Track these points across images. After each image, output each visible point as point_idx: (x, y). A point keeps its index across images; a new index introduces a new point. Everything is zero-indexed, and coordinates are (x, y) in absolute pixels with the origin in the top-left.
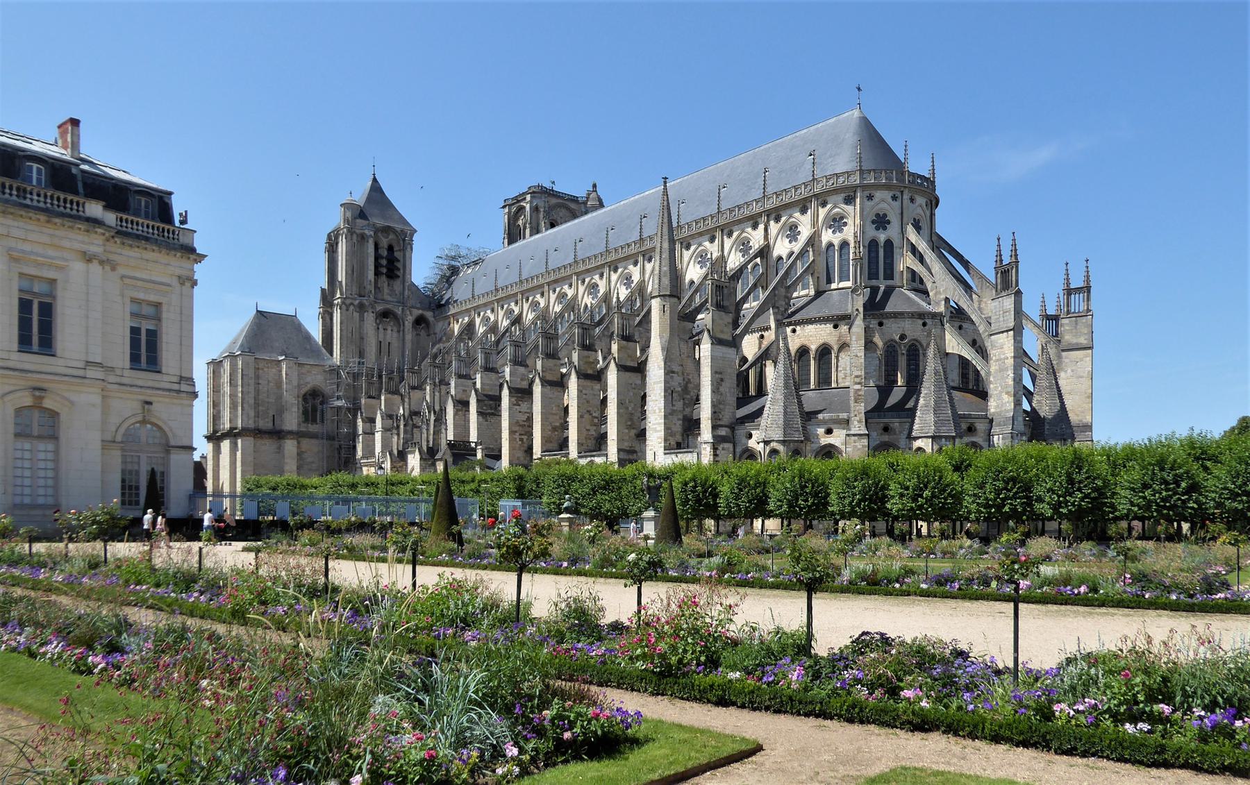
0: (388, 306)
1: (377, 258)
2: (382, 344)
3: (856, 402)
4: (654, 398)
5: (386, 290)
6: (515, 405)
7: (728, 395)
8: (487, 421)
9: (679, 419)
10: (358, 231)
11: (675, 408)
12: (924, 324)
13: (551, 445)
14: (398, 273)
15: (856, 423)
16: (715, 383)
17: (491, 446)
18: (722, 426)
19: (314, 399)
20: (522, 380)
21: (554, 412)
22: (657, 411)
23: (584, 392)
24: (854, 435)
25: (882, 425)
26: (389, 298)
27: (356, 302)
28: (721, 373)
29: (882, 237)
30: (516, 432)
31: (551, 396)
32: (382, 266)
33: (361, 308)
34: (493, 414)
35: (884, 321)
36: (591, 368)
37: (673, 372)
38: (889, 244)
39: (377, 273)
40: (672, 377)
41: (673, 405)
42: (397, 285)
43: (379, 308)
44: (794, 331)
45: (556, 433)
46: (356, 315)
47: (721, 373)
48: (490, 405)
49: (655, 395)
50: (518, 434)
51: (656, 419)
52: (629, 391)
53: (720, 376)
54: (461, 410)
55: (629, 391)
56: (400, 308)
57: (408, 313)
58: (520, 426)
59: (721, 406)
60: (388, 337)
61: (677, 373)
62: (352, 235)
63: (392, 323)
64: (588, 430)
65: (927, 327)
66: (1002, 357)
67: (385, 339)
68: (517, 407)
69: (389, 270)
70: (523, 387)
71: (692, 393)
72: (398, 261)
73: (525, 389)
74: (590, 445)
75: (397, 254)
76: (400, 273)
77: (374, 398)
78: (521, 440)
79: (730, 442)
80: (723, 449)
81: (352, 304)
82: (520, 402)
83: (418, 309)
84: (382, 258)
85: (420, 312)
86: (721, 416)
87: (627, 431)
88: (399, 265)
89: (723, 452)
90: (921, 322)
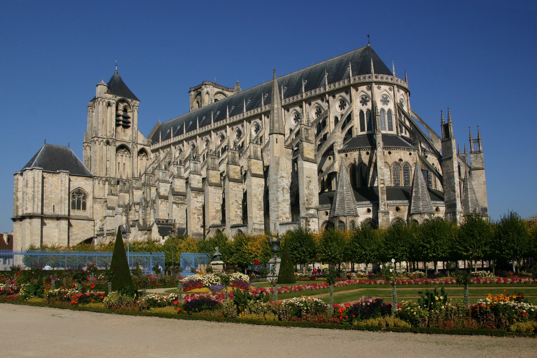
0: (123, 143)
2: (120, 164)
4: (273, 192)
5: (123, 134)
6: (194, 197)
7: (314, 190)
9: (287, 205)
10: (106, 100)
11: (285, 198)
14: (129, 125)
16: (307, 183)
17: (182, 222)
18: (311, 208)
19: (79, 196)
20: (198, 183)
21: (217, 201)
22: (275, 200)
23: (233, 189)
26: (124, 138)
27: (105, 140)
30: (195, 213)
31: (215, 192)
32: (120, 121)
34: (182, 204)
36: (237, 175)
37: (283, 177)
39: (117, 125)
40: (282, 180)
41: (284, 196)
42: (129, 131)
43: (118, 144)
45: (218, 214)
47: (309, 178)
48: (180, 198)
49: (273, 190)
50: (196, 215)
51: (275, 204)
52: (258, 188)
53: (309, 179)
54: (164, 201)
55: (258, 188)
56: (131, 144)
57: (135, 146)
58: (198, 210)
59: (311, 197)
61: (286, 178)
62: (103, 102)
63: (126, 153)
64: (237, 212)
67: (122, 161)
68: (196, 199)
69: (123, 122)
70: (199, 187)
71: (294, 190)
73: (200, 188)
74: (238, 220)
75: (130, 114)
76: (131, 125)
77: (115, 195)
78: (199, 218)
79: (316, 218)
80: (313, 222)
82: (197, 196)
83: (141, 145)
84: (120, 116)
85: (142, 146)
86: (311, 202)
87: (258, 212)
88: (130, 120)
89: (313, 223)
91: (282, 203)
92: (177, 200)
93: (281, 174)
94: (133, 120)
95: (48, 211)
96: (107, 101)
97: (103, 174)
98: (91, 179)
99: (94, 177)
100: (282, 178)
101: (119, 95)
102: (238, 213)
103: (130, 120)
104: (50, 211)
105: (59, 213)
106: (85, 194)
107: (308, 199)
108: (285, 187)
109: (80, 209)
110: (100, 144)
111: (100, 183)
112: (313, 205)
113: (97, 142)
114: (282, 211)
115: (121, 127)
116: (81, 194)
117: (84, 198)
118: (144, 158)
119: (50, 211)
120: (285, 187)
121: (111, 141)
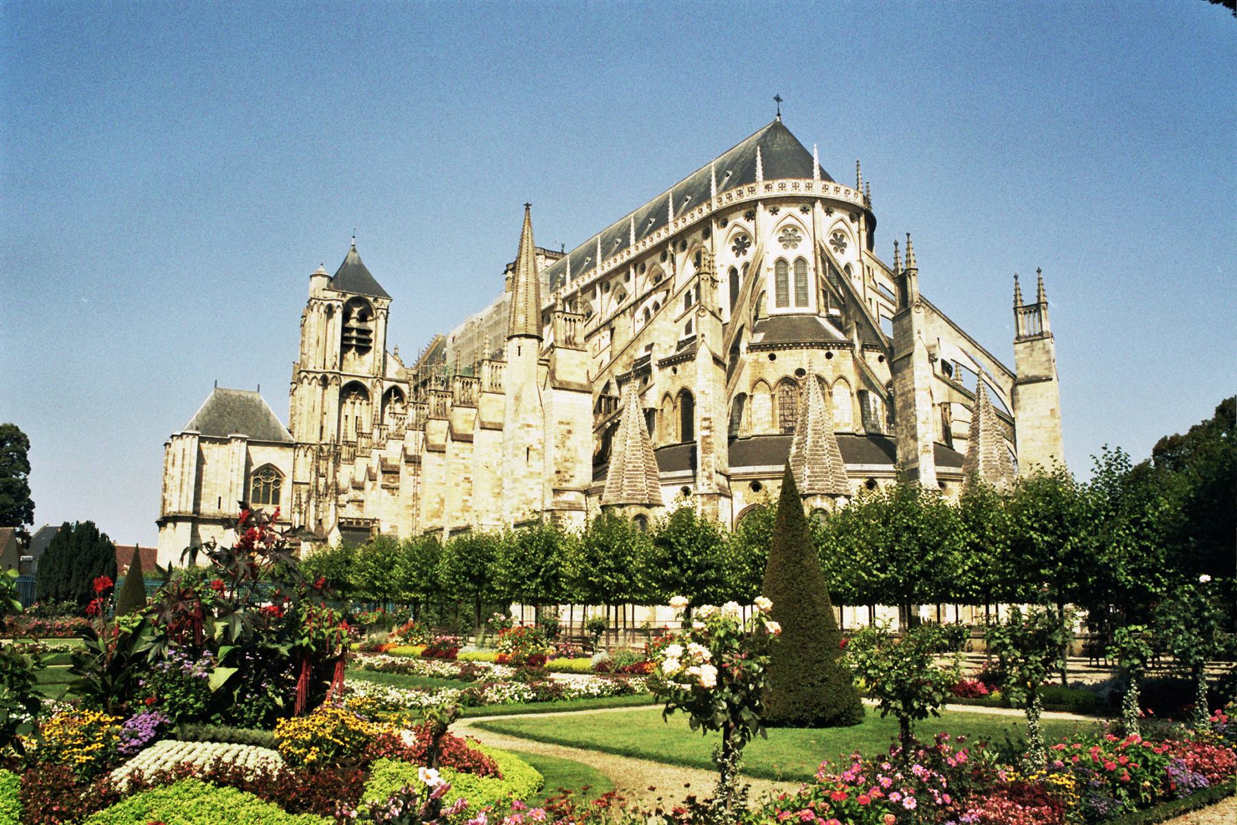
1: (345, 329)
3: (704, 451)
8: (393, 495)
12: (829, 356)
13: (438, 520)
15: (705, 480)
16: (559, 437)
23: (461, 455)
24: (702, 495)
25: (749, 482)
26: (358, 369)
27: (319, 376)
28: (568, 424)
29: (791, 255)
33: (325, 382)
35: (776, 353)
37: (529, 426)
38: (800, 260)
39: (345, 348)
42: (368, 357)
43: (345, 381)
44: (675, 371)
46: (320, 389)
47: (568, 424)
53: (567, 427)
59: (568, 464)
60: (356, 410)
64: (467, 501)
65: (832, 359)
66: (906, 389)
69: (358, 340)
72: (371, 331)
81: (315, 377)
83: (391, 380)
85: (393, 383)
87: (493, 500)
90: (823, 352)
91: (523, 480)
92: (392, 480)
93: (524, 419)
94: (376, 336)
95: (207, 508)
96: (326, 303)
97: (314, 438)
98: (292, 449)
99: (297, 443)
100: (526, 428)
101: (350, 290)
102: (468, 504)
103: (372, 336)
104: (212, 508)
105: (227, 512)
106: (278, 476)
107: (562, 470)
108: (534, 447)
109: (268, 503)
110: (310, 384)
111: (308, 454)
112: (575, 484)
113: (305, 381)
114: (523, 498)
115: (353, 350)
116: (272, 475)
117: (277, 482)
118: (365, 402)
119: (212, 508)
120: (534, 447)
121: (330, 376)
